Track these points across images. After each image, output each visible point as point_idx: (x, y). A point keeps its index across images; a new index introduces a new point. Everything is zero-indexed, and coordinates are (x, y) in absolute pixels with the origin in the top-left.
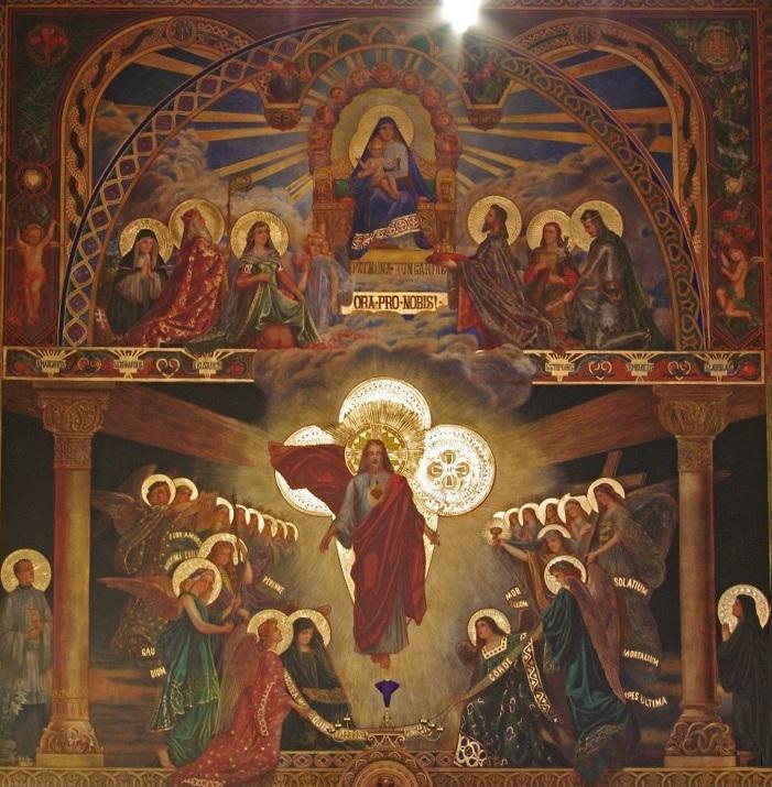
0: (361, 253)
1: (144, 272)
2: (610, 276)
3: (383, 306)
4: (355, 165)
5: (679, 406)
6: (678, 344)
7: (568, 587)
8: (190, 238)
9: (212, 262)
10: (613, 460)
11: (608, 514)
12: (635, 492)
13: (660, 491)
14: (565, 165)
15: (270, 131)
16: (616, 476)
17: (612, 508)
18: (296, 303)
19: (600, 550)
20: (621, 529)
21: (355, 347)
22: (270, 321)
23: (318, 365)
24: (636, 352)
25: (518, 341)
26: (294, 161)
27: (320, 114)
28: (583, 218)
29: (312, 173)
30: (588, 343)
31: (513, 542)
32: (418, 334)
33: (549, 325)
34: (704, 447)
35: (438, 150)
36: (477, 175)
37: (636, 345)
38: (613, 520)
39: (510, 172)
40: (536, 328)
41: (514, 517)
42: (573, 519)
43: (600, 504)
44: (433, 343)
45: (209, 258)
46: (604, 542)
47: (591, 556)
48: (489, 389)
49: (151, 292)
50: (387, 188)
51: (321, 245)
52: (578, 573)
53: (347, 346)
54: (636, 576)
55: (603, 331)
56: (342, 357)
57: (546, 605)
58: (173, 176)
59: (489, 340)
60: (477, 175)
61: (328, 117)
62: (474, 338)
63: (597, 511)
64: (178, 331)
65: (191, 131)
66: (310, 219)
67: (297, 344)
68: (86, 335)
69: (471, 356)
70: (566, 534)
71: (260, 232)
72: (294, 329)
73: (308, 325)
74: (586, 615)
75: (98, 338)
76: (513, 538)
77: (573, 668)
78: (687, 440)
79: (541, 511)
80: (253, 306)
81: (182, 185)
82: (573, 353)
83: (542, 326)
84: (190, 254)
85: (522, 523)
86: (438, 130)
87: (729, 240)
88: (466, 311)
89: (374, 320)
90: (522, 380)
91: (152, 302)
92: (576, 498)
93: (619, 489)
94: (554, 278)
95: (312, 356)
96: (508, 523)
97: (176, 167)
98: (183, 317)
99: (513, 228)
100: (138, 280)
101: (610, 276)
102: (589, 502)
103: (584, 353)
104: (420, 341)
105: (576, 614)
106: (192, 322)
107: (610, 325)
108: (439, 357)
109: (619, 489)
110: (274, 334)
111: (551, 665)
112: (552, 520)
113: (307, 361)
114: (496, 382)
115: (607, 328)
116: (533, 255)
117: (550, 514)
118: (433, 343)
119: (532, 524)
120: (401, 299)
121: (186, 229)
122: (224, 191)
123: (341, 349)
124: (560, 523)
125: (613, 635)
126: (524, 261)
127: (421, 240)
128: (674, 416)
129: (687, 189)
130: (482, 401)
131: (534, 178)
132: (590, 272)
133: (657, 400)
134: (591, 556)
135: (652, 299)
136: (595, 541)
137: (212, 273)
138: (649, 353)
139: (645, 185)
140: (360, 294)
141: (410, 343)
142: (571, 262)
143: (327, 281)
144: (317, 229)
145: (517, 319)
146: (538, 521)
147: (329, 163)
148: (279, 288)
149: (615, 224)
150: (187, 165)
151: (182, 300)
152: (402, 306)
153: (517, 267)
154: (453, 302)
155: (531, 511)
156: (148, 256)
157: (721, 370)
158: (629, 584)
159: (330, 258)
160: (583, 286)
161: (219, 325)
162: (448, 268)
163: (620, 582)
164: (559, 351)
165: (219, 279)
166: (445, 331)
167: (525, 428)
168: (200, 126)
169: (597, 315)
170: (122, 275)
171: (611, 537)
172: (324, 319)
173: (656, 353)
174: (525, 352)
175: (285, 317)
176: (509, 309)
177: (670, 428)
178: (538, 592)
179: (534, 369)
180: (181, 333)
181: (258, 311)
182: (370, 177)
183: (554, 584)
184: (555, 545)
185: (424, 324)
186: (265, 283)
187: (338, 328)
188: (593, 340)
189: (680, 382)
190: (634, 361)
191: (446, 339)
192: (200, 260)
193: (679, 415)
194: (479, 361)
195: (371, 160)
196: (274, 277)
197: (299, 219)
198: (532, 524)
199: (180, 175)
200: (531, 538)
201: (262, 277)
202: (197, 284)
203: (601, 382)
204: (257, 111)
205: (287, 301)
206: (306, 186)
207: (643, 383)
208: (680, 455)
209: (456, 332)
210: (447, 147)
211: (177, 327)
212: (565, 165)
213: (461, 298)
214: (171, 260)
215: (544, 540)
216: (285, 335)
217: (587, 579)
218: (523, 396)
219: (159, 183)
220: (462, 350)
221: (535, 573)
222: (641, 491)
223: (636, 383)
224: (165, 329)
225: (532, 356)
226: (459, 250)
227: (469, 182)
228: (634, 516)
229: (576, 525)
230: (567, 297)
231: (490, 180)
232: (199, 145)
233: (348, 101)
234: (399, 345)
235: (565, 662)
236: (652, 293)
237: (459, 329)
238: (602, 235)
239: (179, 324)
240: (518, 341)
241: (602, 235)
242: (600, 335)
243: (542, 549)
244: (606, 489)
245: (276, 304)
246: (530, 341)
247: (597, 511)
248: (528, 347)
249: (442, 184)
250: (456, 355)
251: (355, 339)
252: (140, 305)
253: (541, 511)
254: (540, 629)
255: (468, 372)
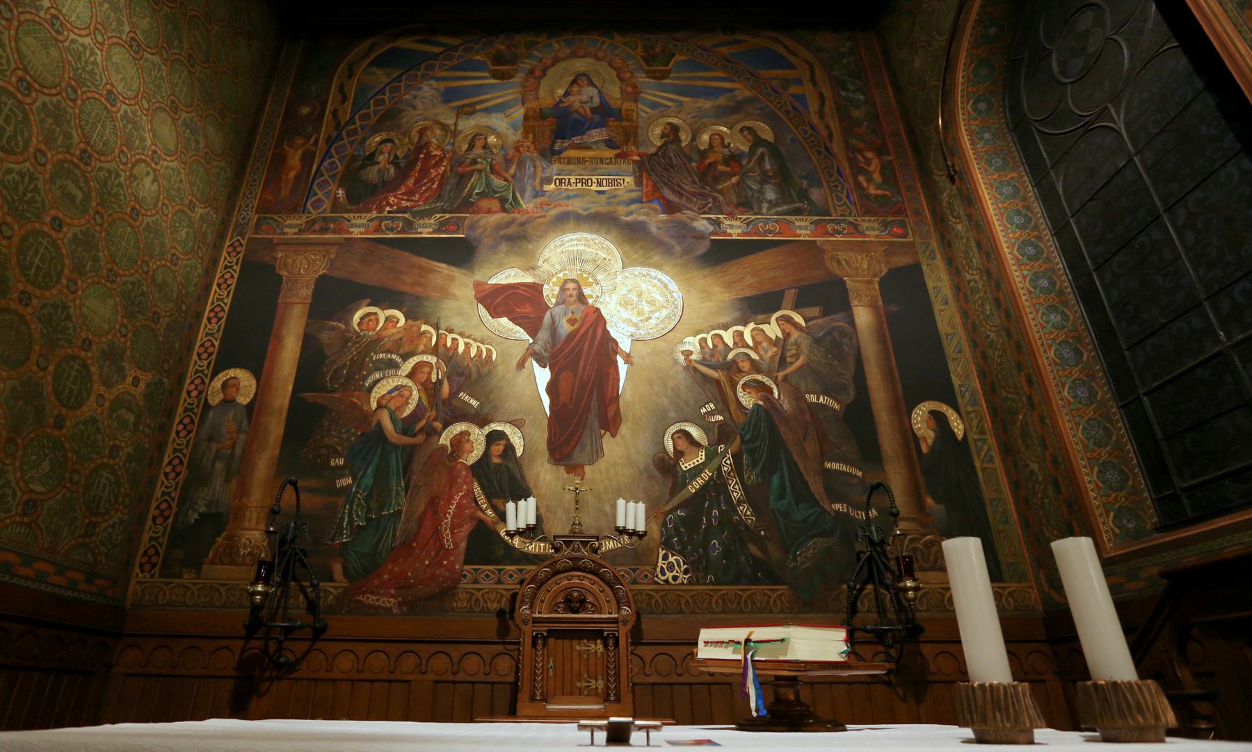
0: (560, 152)
1: (381, 165)
2: (768, 167)
3: (579, 185)
4: (558, 100)
5: (842, 256)
6: (832, 211)
7: (761, 403)
8: (422, 143)
9: (438, 158)
10: (790, 295)
11: (792, 339)
12: (815, 322)
13: (838, 321)
14: (722, 100)
15: (492, 81)
16: (796, 307)
17: (795, 335)
18: (506, 183)
19: (790, 370)
20: (805, 351)
21: (554, 212)
22: (482, 195)
23: (522, 225)
24: (798, 217)
25: (695, 209)
26: (510, 97)
27: (531, 72)
28: (741, 131)
29: (523, 104)
30: (756, 210)
31: (703, 362)
32: (609, 204)
33: (721, 198)
34: (871, 286)
35: (622, 91)
36: (654, 105)
37: (797, 212)
38: (797, 344)
39: (681, 104)
40: (710, 200)
41: (704, 341)
42: (760, 343)
43: (783, 331)
44: (622, 210)
45: (436, 155)
46: (792, 363)
47: (781, 375)
48: (673, 242)
49: (386, 176)
50: (583, 113)
51: (529, 147)
52: (770, 391)
53: (547, 212)
54: (826, 392)
55: (767, 202)
56: (542, 219)
57: (742, 419)
58: (415, 108)
59: (670, 208)
60: (654, 105)
61: (537, 73)
62: (657, 206)
63: (780, 335)
64: (403, 202)
65: (433, 82)
66: (520, 132)
67: (504, 210)
68: (327, 204)
69: (655, 220)
70: (754, 356)
71: (479, 139)
72: (503, 200)
73: (514, 197)
74: (782, 429)
75: (336, 206)
76: (704, 359)
77: (776, 479)
78: (854, 281)
79: (728, 337)
80: (469, 185)
81: (420, 112)
82: (744, 217)
83: (715, 199)
84: (421, 153)
85: (711, 346)
86: (622, 80)
87: (861, 145)
88: (649, 188)
89: (571, 194)
90: (701, 236)
91: (385, 183)
92: (761, 326)
93: (799, 319)
94: (721, 168)
95: (517, 219)
96: (698, 347)
97: (418, 102)
98: (410, 193)
99: (685, 137)
100: (376, 170)
101: (768, 167)
102: (773, 330)
103: (753, 217)
104: (611, 208)
105: (773, 429)
106: (416, 198)
107: (773, 199)
108: (629, 219)
109: (799, 319)
110: (485, 204)
111: (752, 477)
112: (740, 344)
113: (513, 221)
114: (681, 238)
115: (771, 201)
116: (703, 154)
117: (737, 339)
118: (622, 210)
119: (721, 347)
120: (595, 180)
121: (420, 139)
122: (453, 115)
123: (542, 214)
124: (748, 346)
125: (811, 447)
126: (695, 156)
127: (610, 144)
128: (839, 262)
129: (822, 115)
130: (667, 251)
131: (699, 108)
132: (752, 164)
133: (823, 251)
134: (781, 375)
135: (805, 182)
136: (783, 362)
137: (438, 164)
138: (809, 218)
139: (788, 112)
140: (560, 177)
141: (603, 209)
142: (733, 159)
143: (532, 169)
144: (526, 137)
145: (694, 194)
146: (726, 345)
147: (537, 98)
148: (492, 173)
149: (767, 133)
150: (425, 100)
151: (411, 182)
152: (594, 185)
153: (690, 160)
154: (639, 182)
155: (720, 337)
156: (387, 155)
157: (874, 230)
158: (821, 399)
159: (535, 155)
160: (746, 173)
161: (439, 198)
162: (633, 161)
163: (812, 398)
164: (731, 215)
165: (443, 168)
166: (633, 201)
167: (707, 271)
168: (438, 79)
169: (761, 192)
170: (363, 166)
171: (797, 359)
172: (528, 193)
173: (817, 218)
174: (702, 216)
175: (495, 192)
176: (686, 187)
177: (838, 272)
178: (733, 407)
179: (711, 228)
180: (405, 204)
181: (473, 189)
182: (570, 106)
183: (748, 400)
184: (745, 366)
185: (615, 197)
186: (480, 171)
187: (539, 200)
188: (760, 208)
189: (839, 238)
190: (798, 224)
191: (633, 207)
192: (429, 156)
193: (844, 263)
194: (663, 222)
195: (570, 97)
196: (488, 167)
197: (511, 131)
198: (721, 347)
199: (420, 106)
200: (721, 359)
201: (478, 166)
202: (424, 172)
203: (770, 237)
204: (485, 71)
205: (497, 182)
206: (519, 113)
207: (808, 239)
208: (850, 293)
209: (641, 202)
210: (630, 89)
211: (403, 200)
212: (722, 100)
213: (645, 180)
214: (406, 157)
215: (734, 361)
216: (495, 205)
217: (779, 395)
218: (703, 248)
219: (402, 111)
220: (648, 214)
221: (728, 390)
222: (820, 321)
223: (802, 238)
224: (393, 201)
225: (708, 219)
226: (642, 150)
227: (648, 110)
228: (817, 341)
229: (763, 348)
230: (734, 180)
231: (663, 109)
232: (437, 90)
233: (553, 65)
234: (593, 210)
235: (767, 473)
236: (805, 178)
237: (644, 200)
238: (758, 142)
239: (405, 198)
240: (695, 209)
241: (758, 142)
242: (765, 205)
243: (732, 368)
244: (789, 320)
245: (488, 184)
246: (706, 209)
247: (780, 335)
248: (705, 213)
249: (626, 111)
250: (642, 218)
251: (555, 207)
252: (375, 186)
253: (728, 337)
254: (738, 441)
255: (654, 229)
